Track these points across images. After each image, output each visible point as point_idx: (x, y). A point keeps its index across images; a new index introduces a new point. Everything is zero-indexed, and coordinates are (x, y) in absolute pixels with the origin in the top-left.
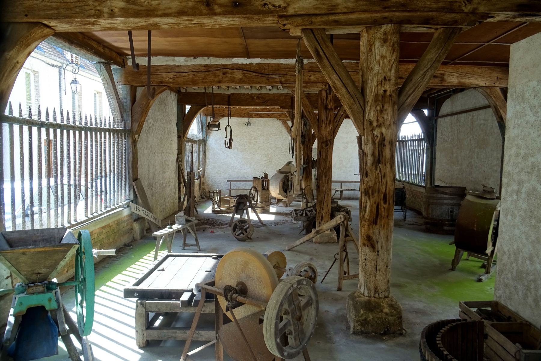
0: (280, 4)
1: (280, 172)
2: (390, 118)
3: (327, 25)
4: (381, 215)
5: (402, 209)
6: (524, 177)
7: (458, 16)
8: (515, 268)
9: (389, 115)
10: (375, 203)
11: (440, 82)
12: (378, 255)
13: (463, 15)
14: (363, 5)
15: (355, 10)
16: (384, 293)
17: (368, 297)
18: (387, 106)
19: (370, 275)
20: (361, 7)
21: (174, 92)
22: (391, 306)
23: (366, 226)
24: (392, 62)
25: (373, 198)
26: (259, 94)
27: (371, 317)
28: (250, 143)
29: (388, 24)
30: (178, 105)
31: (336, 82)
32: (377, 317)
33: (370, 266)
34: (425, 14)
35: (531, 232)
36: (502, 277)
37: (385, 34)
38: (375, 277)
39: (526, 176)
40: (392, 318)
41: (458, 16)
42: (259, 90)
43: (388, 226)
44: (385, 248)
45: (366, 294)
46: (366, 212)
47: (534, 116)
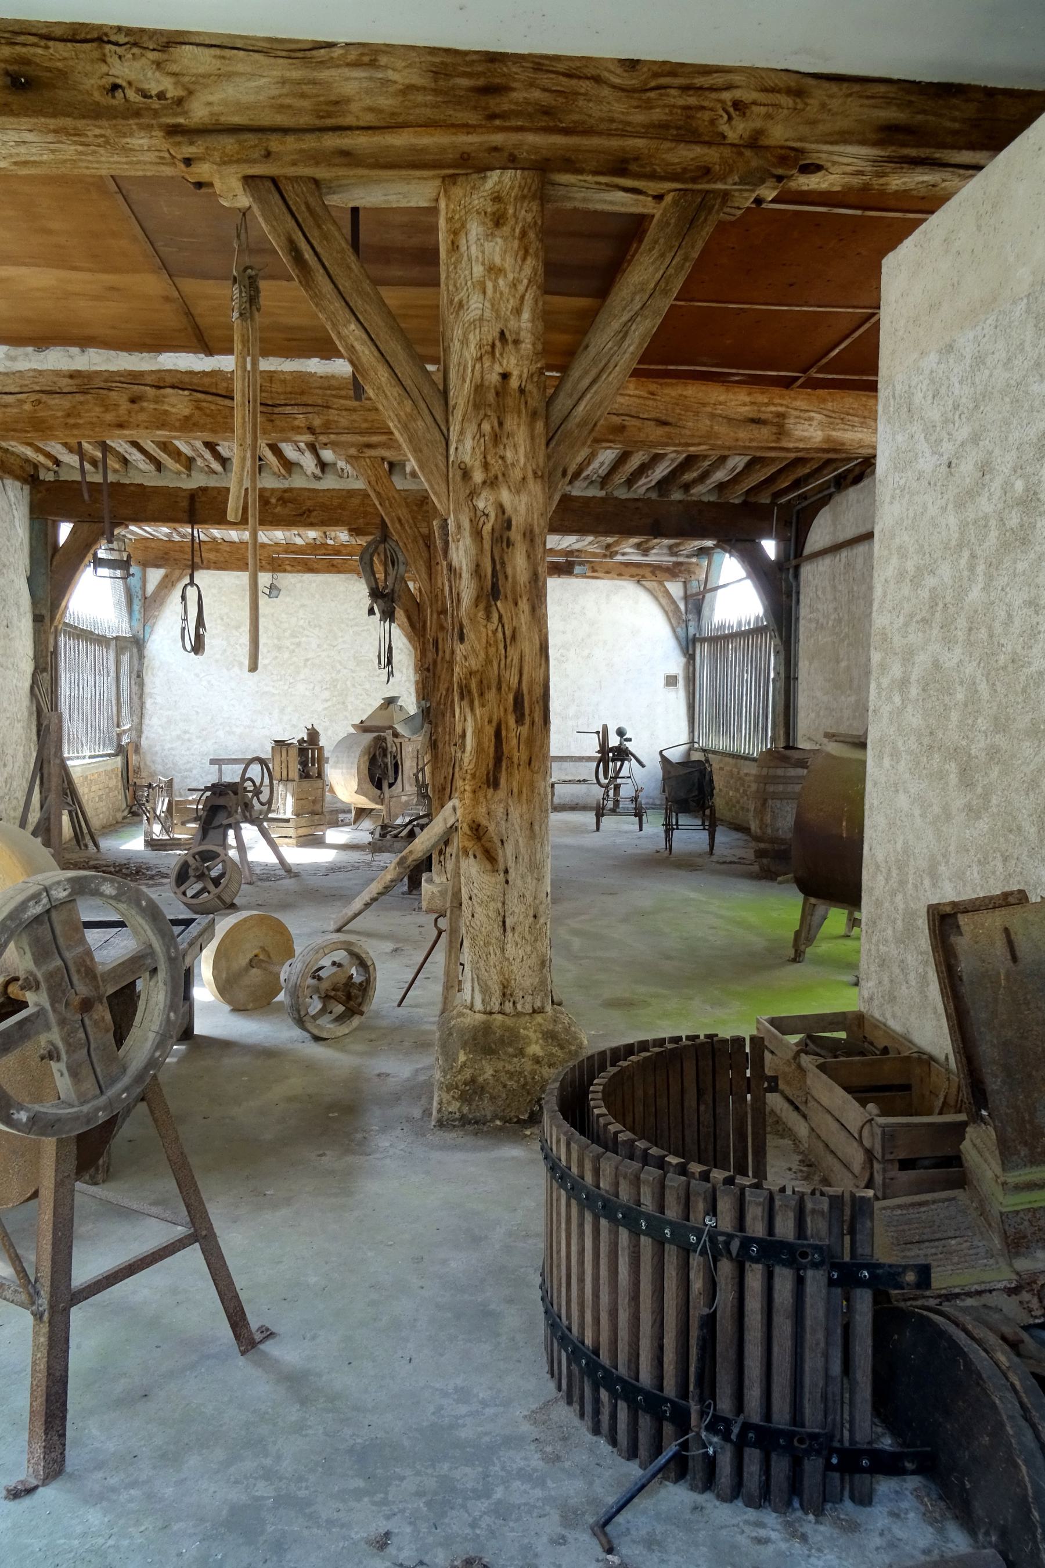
0: (161, 88)
1: (363, 728)
2: (522, 461)
3: (317, 164)
4: (510, 759)
5: (703, 824)
6: (915, 638)
7: (711, 155)
8: (901, 906)
9: (522, 451)
10: (490, 722)
11: (774, 437)
12: (507, 882)
13: (727, 152)
14: (426, 106)
15: (400, 120)
16: (529, 998)
17: (485, 1013)
18: (511, 423)
19: (487, 944)
20: (417, 111)
21: (17, 478)
22: (550, 1036)
23: (467, 795)
24: (521, 288)
25: (483, 706)
26: (286, 491)
27: (489, 1072)
28: (279, 648)
29: (504, 168)
30: (32, 519)
31: (358, 346)
32: (507, 1072)
33: (485, 919)
34: (615, 143)
35: (931, 794)
36: (875, 939)
37: (497, 199)
38: (503, 950)
39: (920, 634)
40: (552, 1071)
41: (711, 155)
42: (285, 477)
43: (533, 792)
44: (526, 857)
45: (479, 1006)
46: (463, 752)
47: (934, 453)
